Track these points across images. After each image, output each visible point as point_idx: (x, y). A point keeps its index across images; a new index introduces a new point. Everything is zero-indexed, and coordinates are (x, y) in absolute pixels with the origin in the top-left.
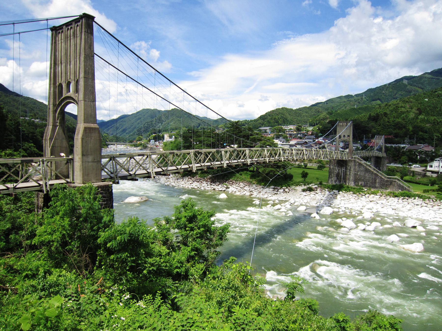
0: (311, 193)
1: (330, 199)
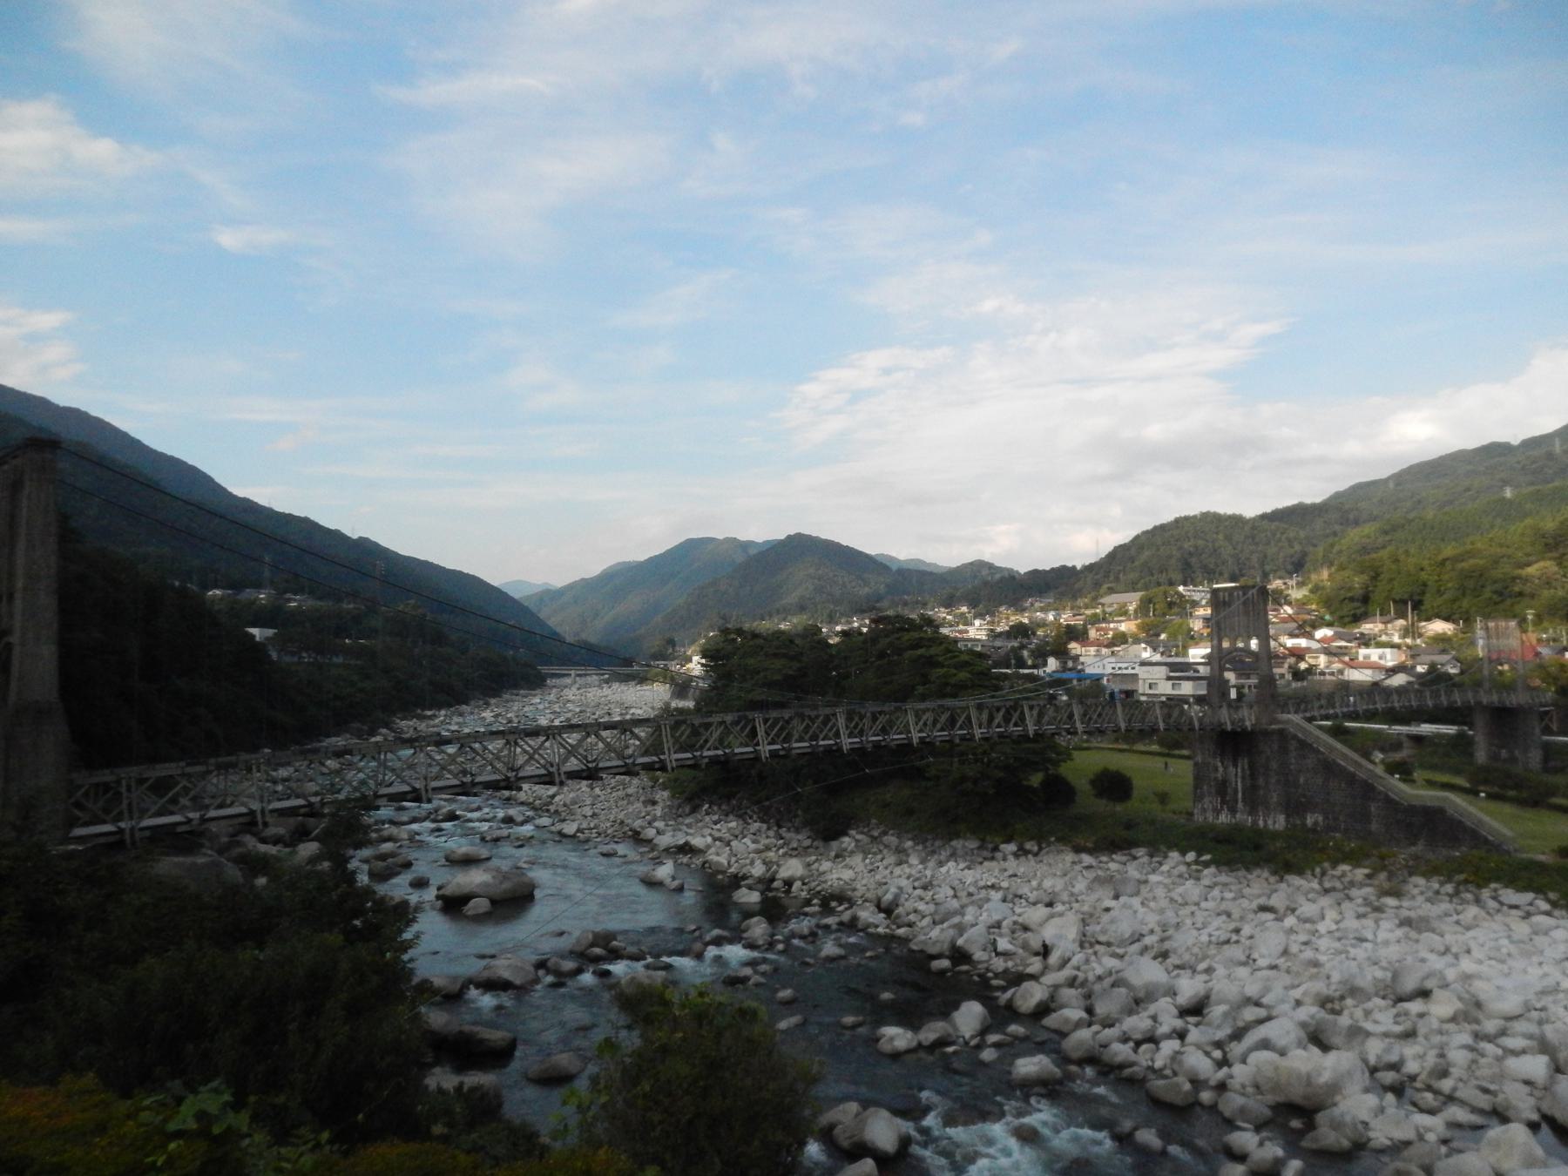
0: (1114, 856)
1: (1177, 880)
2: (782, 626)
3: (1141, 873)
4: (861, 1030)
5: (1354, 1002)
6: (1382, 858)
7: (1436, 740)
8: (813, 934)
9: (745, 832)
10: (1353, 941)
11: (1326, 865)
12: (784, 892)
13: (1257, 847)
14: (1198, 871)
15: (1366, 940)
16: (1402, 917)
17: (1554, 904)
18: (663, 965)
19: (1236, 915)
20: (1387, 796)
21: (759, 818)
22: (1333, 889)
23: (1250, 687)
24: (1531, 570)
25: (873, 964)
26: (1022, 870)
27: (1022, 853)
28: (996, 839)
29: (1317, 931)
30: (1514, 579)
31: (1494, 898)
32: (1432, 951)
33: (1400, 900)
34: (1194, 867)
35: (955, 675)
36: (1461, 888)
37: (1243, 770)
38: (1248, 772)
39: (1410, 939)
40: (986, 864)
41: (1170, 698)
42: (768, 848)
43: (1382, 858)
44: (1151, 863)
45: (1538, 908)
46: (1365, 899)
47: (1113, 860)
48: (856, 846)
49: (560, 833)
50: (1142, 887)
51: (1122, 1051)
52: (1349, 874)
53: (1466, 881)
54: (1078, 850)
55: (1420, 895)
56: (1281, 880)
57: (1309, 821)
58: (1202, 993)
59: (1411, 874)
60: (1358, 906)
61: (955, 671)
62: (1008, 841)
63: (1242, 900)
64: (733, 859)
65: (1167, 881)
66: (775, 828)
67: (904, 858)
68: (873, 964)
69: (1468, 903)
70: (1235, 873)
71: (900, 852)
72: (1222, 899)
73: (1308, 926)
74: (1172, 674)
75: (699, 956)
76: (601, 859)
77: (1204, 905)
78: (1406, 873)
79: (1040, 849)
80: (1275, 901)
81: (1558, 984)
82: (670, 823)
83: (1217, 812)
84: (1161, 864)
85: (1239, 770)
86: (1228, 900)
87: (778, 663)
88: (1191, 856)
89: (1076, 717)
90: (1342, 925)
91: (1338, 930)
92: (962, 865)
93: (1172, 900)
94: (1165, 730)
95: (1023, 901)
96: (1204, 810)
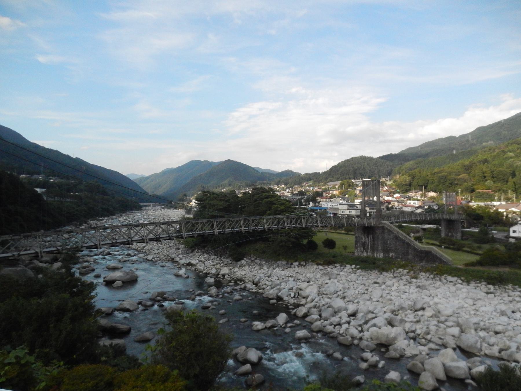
0: (329, 266)
2: (223, 191)
3: (337, 271)
4: (247, 323)
5: (402, 312)
6: (412, 267)
7: (430, 230)
8: (232, 292)
9: (210, 259)
10: (403, 293)
11: (395, 269)
12: (222, 278)
13: (374, 263)
14: (355, 271)
15: (406, 292)
16: (417, 285)
17: (463, 281)
18: (181, 302)
19: (367, 285)
20: (414, 247)
21: (214, 254)
22: (397, 277)
23: (373, 212)
24: (460, 176)
25: (250, 302)
26: (300, 271)
27: (300, 265)
28: (293, 261)
29: (391, 290)
30: (455, 179)
31: (445, 279)
32: (426, 296)
33: (417, 280)
34: (354, 270)
35: (280, 207)
36: (436, 276)
37: (371, 239)
38: (372, 240)
39: (419, 292)
40: (288, 269)
41: (348, 216)
42: (217, 264)
43: (412, 267)
44: (341, 268)
45: (458, 282)
46: (406, 280)
47: (329, 267)
48: (246, 263)
49: (146, 259)
50: (338, 276)
51: (330, 328)
52: (402, 272)
53: (437, 274)
54: (318, 264)
55: (423, 278)
56: (381, 274)
57: (390, 255)
58: (356, 309)
59: (421, 272)
60: (404, 282)
61: (280, 206)
62: (295, 262)
63: (368, 280)
64: (205, 268)
65: (346, 274)
66: (219, 257)
67: (262, 267)
68: (250, 302)
69: (437, 280)
70: (367, 272)
71: (260, 265)
72: (363, 280)
73: (389, 288)
74: (349, 208)
75: (193, 300)
76: (161, 268)
77: (357, 282)
78: (419, 271)
79: (306, 264)
80: (380, 280)
81: (463, 305)
82: (184, 256)
83: (362, 252)
84: (344, 269)
85: (369, 239)
86: (364, 280)
87: (221, 203)
88: (353, 266)
89: (319, 222)
90: (399, 288)
91: (398, 289)
92: (281, 269)
93: (347, 280)
94: (347, 226)
95: (300, 281)
96: (358, 252)
